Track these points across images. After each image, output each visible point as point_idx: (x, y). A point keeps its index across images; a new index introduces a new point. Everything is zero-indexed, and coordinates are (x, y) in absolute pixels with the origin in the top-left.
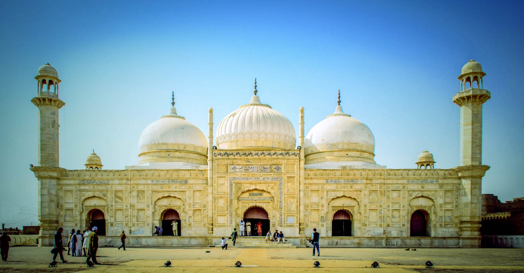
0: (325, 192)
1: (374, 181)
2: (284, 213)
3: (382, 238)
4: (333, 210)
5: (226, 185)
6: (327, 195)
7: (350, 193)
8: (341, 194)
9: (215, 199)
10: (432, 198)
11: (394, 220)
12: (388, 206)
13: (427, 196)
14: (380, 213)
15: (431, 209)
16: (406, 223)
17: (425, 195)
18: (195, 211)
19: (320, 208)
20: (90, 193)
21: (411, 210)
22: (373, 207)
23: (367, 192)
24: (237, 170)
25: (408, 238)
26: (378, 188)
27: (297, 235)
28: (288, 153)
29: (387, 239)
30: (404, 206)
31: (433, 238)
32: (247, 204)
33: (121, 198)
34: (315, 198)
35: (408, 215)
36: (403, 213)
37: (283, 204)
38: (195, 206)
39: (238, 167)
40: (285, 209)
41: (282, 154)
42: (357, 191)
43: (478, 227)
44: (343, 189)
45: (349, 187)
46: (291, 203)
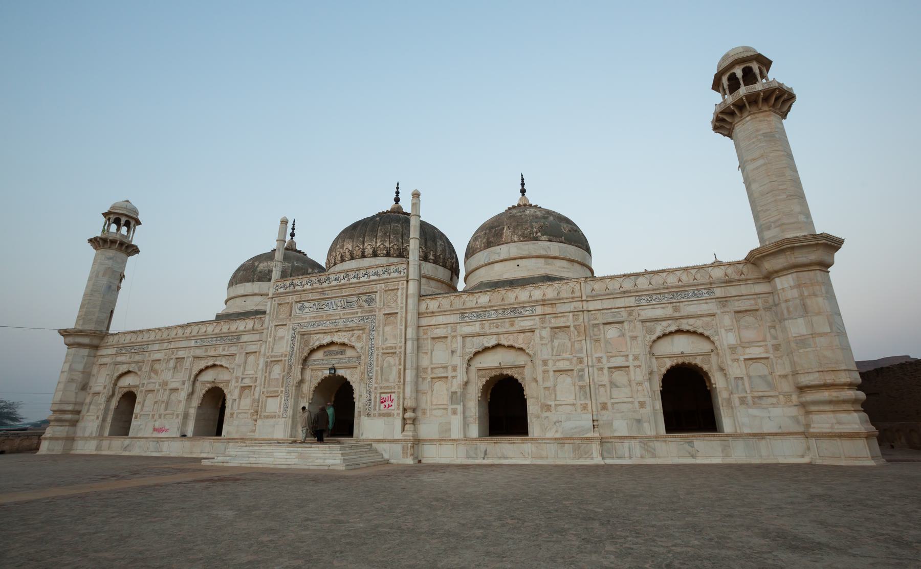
0: (460, 339)
1: (560, 308)
2: (376, 388)
3: (592, 438)
4: (480, 377)
5: (286, 338)
6: (464, 347)
7: (511, 337)
8: (492, 342)
9: (269, 365)
10: (706, 333)
11: (615, 393)
12: (599, 360)
13: (691, 329)
14: (581, 377)
15: (709, 362)
16: (648, 400)
17: (685, 327)
18: (244, 388)
19: (450, 374)
20: (125, 366)
21: (659, 367)
22: (562, 365)
23: (546, 333)
24: (307, 310)
25: (657, 437)
26: (569, 320)
27: (398, 435)
28: (387, 271)
29: (603, 441)
30: (636, 358)
31: (728, 435)
32: (320, 373)
33: (156, 372)
34: (439, 355)
35: (650, 380)
36: (638, 375)
37: (375, 369)
38: (245, 381)
39: (307, 305)
40: (376, 379)
41: (377, 273)
42: (524, 331)
43: (855, 401)
44: (495, 330)
45: (507, 325)
46: (390, 366)
